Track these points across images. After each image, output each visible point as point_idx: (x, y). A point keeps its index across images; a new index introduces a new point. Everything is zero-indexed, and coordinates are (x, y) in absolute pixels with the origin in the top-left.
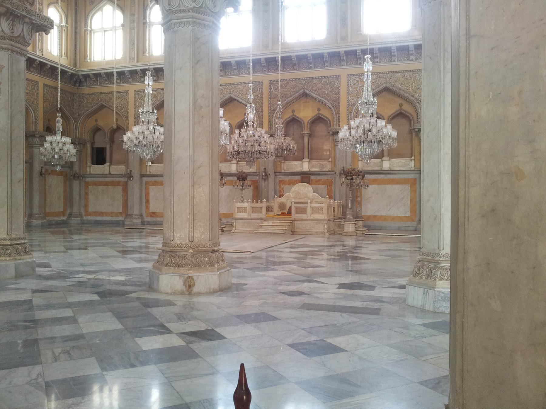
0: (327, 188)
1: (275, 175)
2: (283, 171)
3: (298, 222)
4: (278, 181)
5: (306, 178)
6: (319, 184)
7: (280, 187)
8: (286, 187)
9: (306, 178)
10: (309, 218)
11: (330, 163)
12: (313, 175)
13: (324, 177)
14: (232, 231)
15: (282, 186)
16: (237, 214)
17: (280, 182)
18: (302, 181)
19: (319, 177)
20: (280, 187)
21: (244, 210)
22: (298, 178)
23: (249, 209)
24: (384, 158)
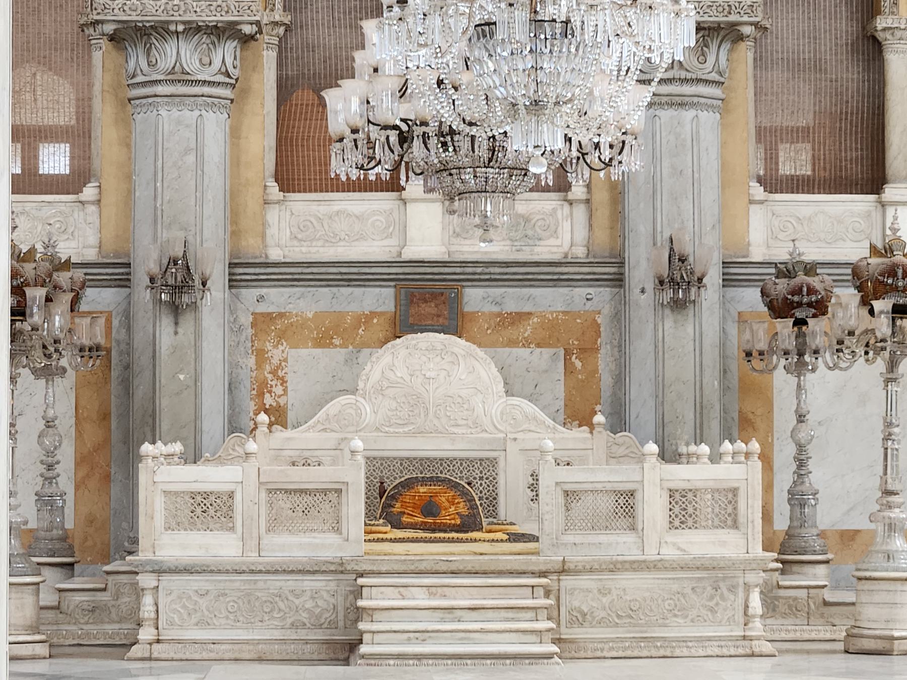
0: (569, 369)
1: (233, 283)
2: (275, 255)
3: (584, 581)
4: (246, 320)
5: (428, 299)
6: (512, 343)
7: (261, 356)
8: (304, 367)
9: (428, 299)
10: (651, 554)
11: (580, 212)
12: (475, 281)
13: (549, 300)
14: (135, 651)
15: (276, 354)
16: (167, 538)
17: (262, 322)
18: (402, 325)
19: (513, 299)
20: (261, 356)
21: (210, 509)
22: (380, 299)
23: (249, 503)
24: (890, 192)
